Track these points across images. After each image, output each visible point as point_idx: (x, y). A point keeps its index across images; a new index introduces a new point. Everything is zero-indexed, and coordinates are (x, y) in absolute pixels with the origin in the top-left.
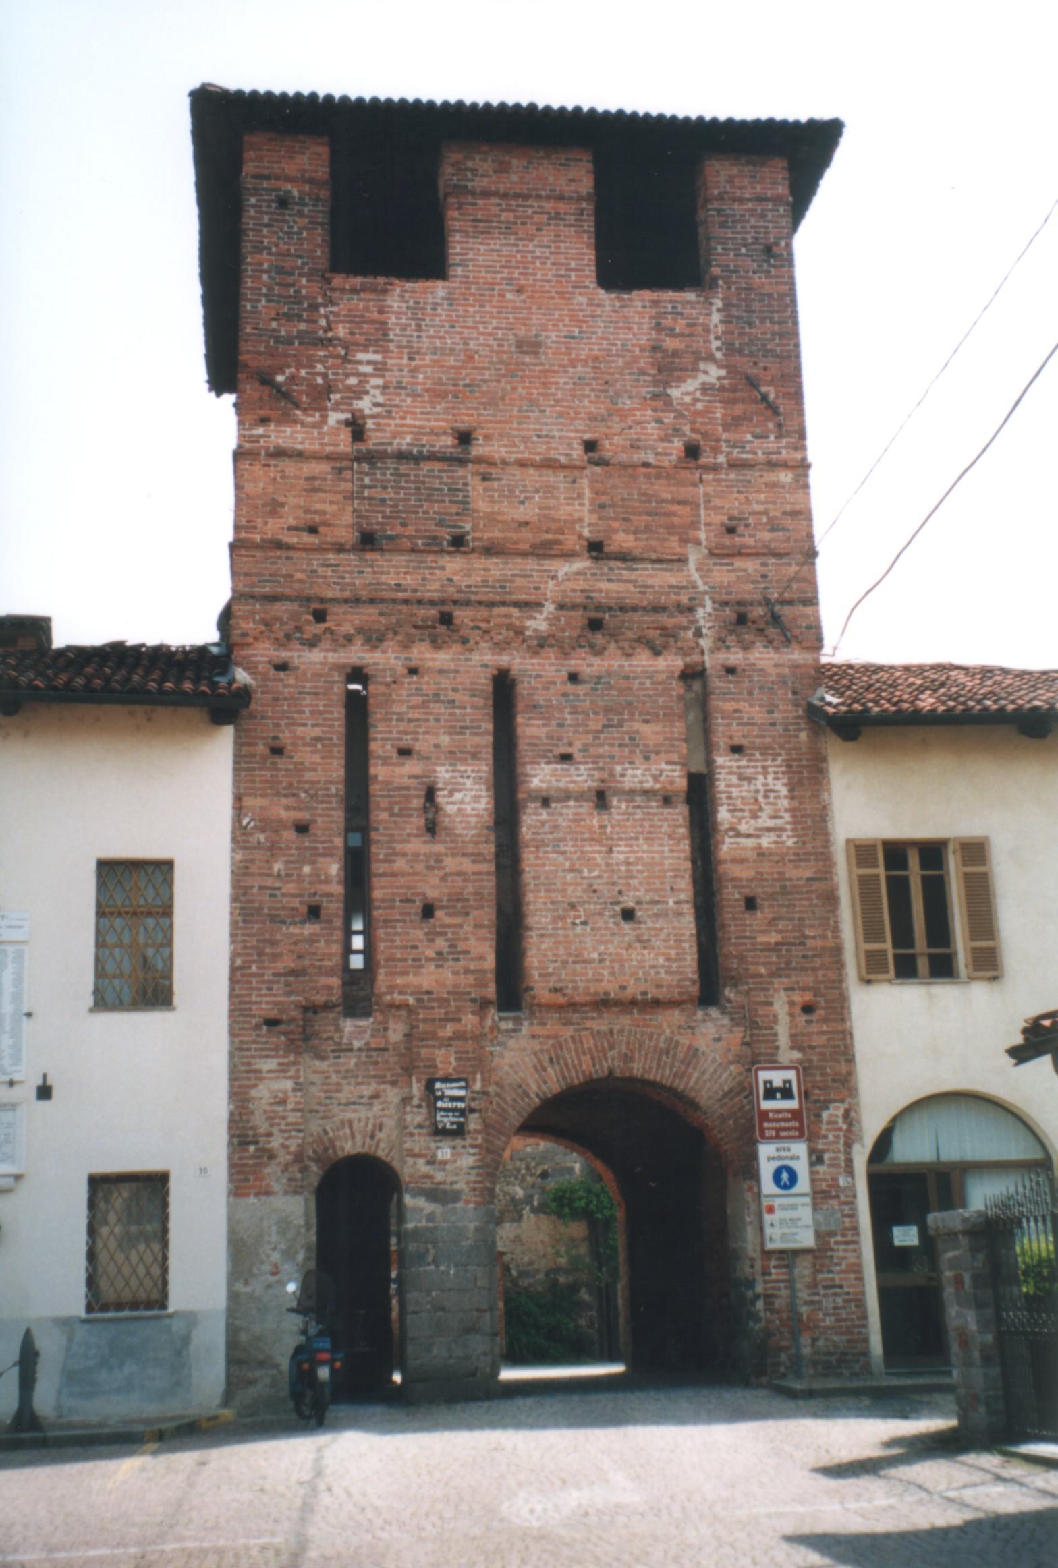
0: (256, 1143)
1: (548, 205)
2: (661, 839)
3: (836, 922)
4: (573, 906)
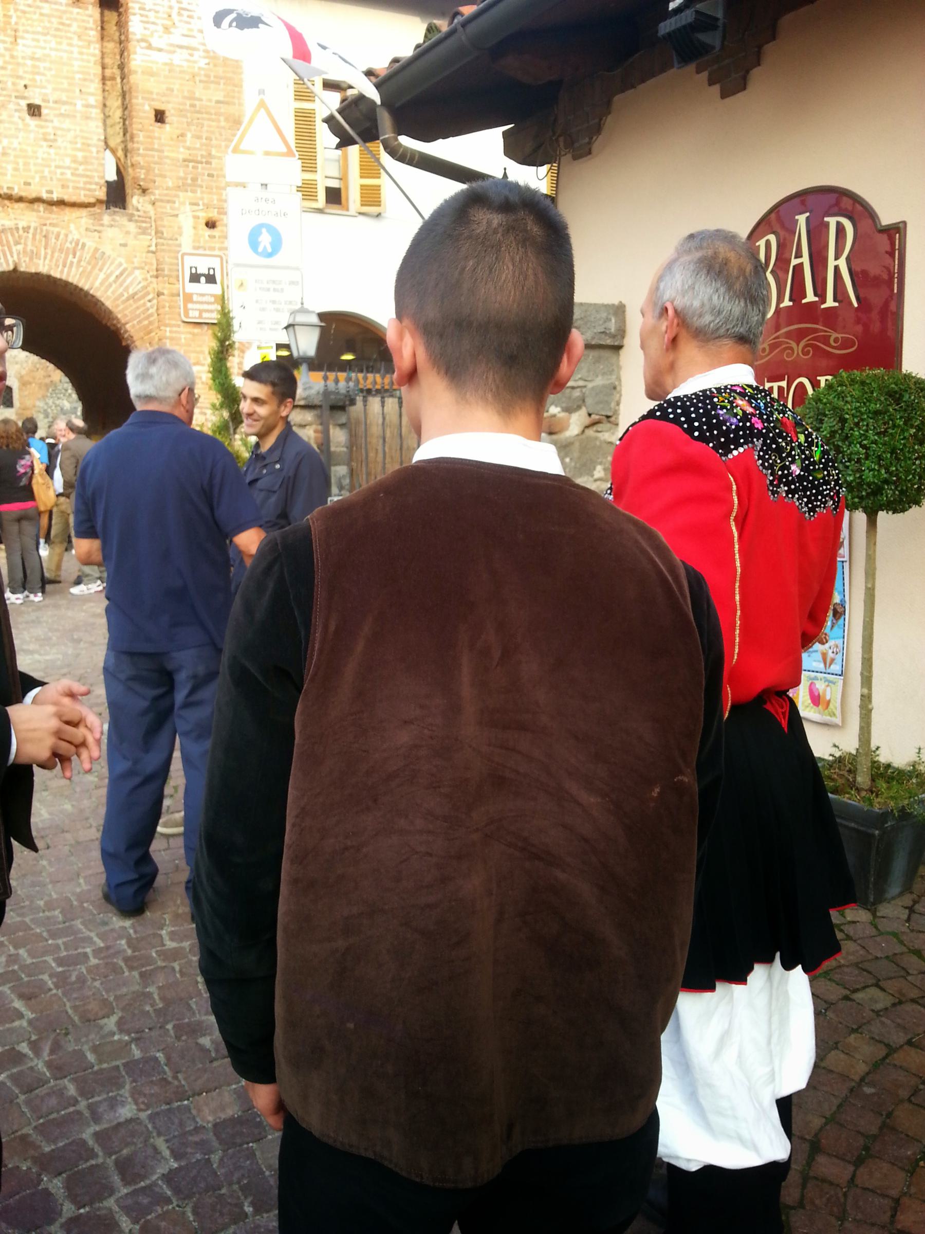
2: (70, 38)
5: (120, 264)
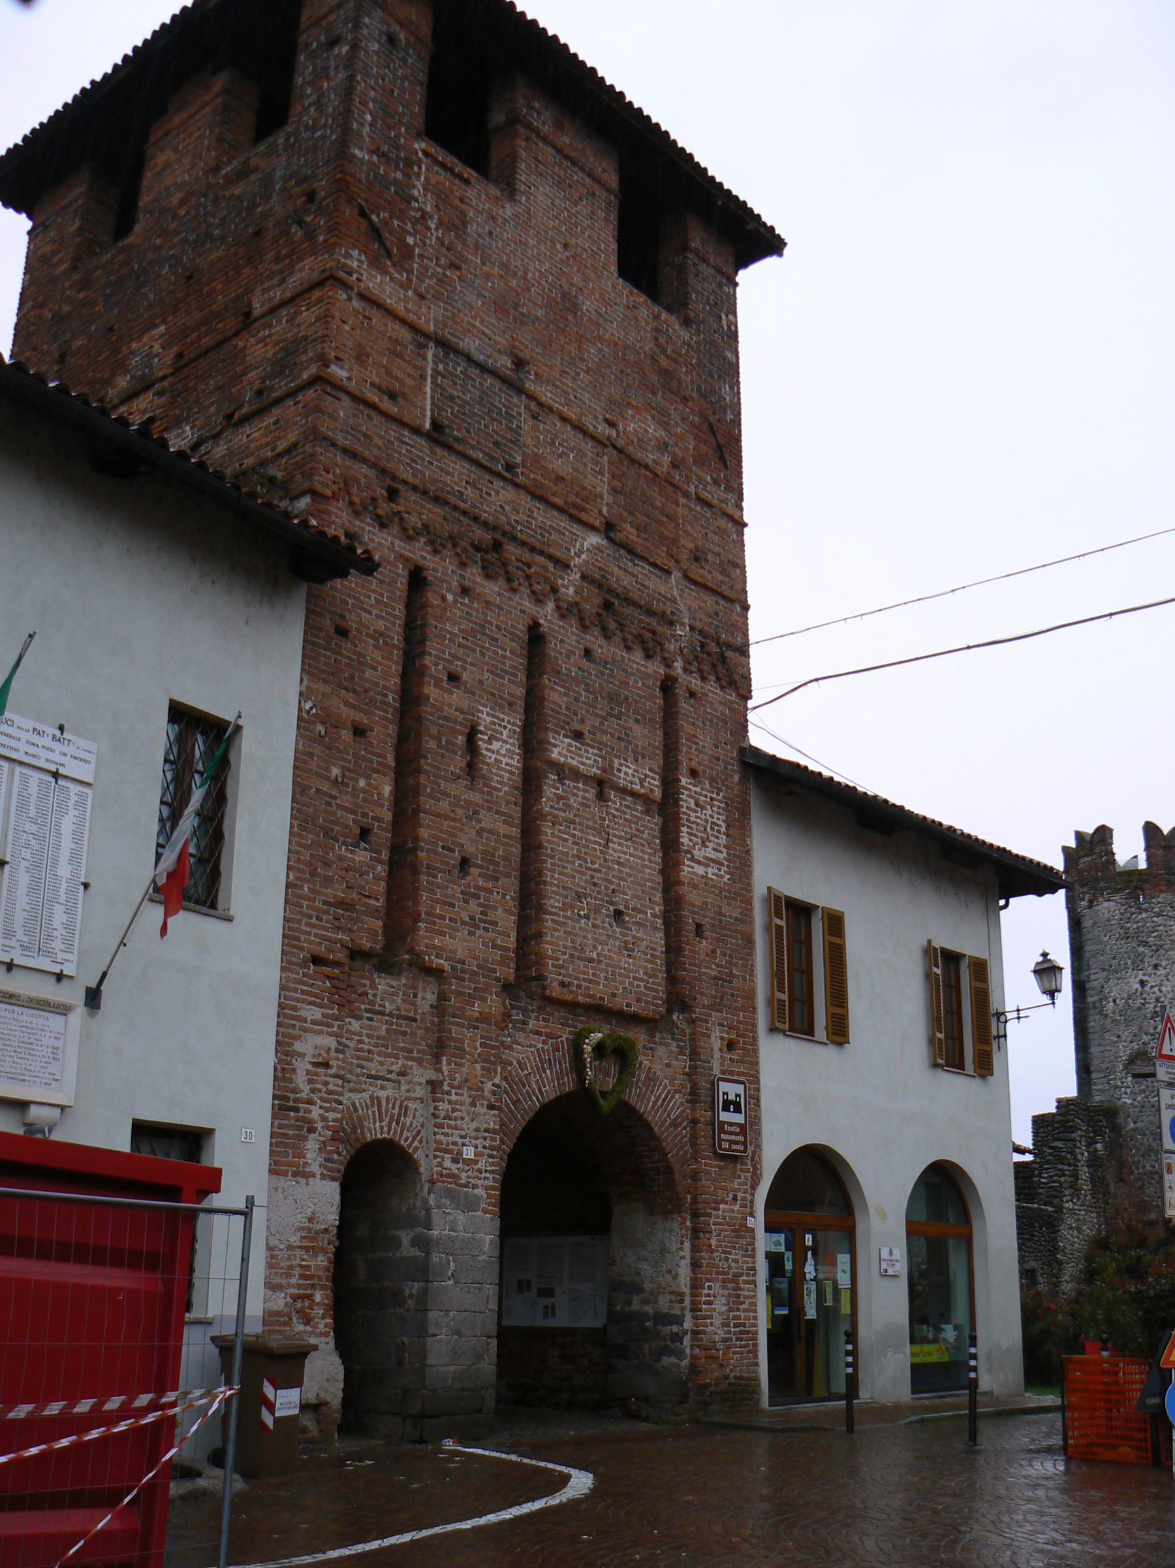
0: (297, 1110)
1: (588, 181)
3: (752, 965)
4: (579, 896)
5: (666, 1085)
